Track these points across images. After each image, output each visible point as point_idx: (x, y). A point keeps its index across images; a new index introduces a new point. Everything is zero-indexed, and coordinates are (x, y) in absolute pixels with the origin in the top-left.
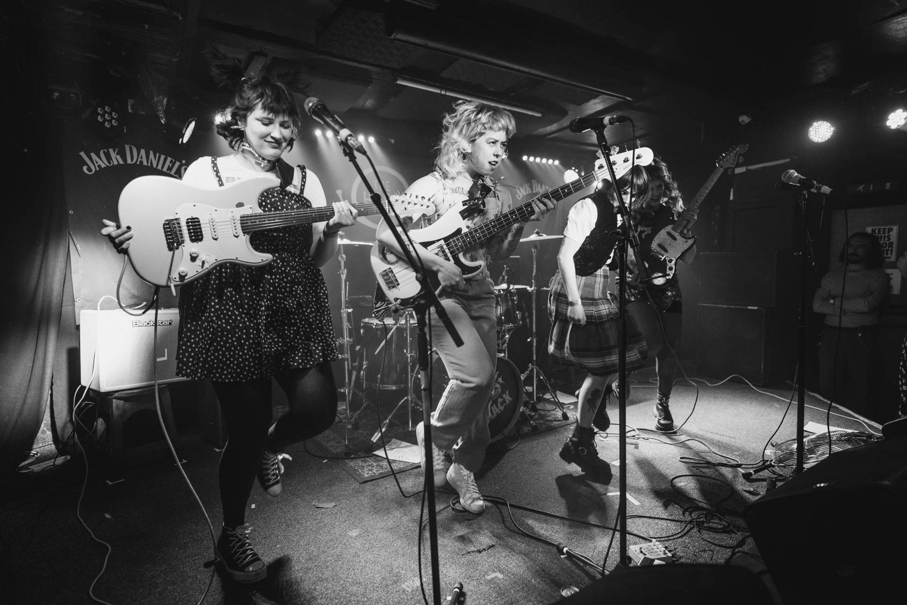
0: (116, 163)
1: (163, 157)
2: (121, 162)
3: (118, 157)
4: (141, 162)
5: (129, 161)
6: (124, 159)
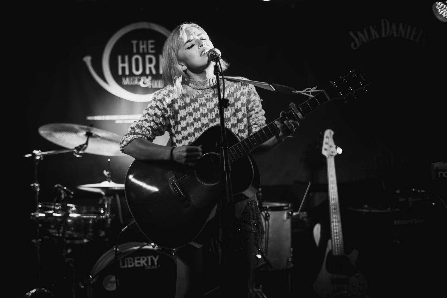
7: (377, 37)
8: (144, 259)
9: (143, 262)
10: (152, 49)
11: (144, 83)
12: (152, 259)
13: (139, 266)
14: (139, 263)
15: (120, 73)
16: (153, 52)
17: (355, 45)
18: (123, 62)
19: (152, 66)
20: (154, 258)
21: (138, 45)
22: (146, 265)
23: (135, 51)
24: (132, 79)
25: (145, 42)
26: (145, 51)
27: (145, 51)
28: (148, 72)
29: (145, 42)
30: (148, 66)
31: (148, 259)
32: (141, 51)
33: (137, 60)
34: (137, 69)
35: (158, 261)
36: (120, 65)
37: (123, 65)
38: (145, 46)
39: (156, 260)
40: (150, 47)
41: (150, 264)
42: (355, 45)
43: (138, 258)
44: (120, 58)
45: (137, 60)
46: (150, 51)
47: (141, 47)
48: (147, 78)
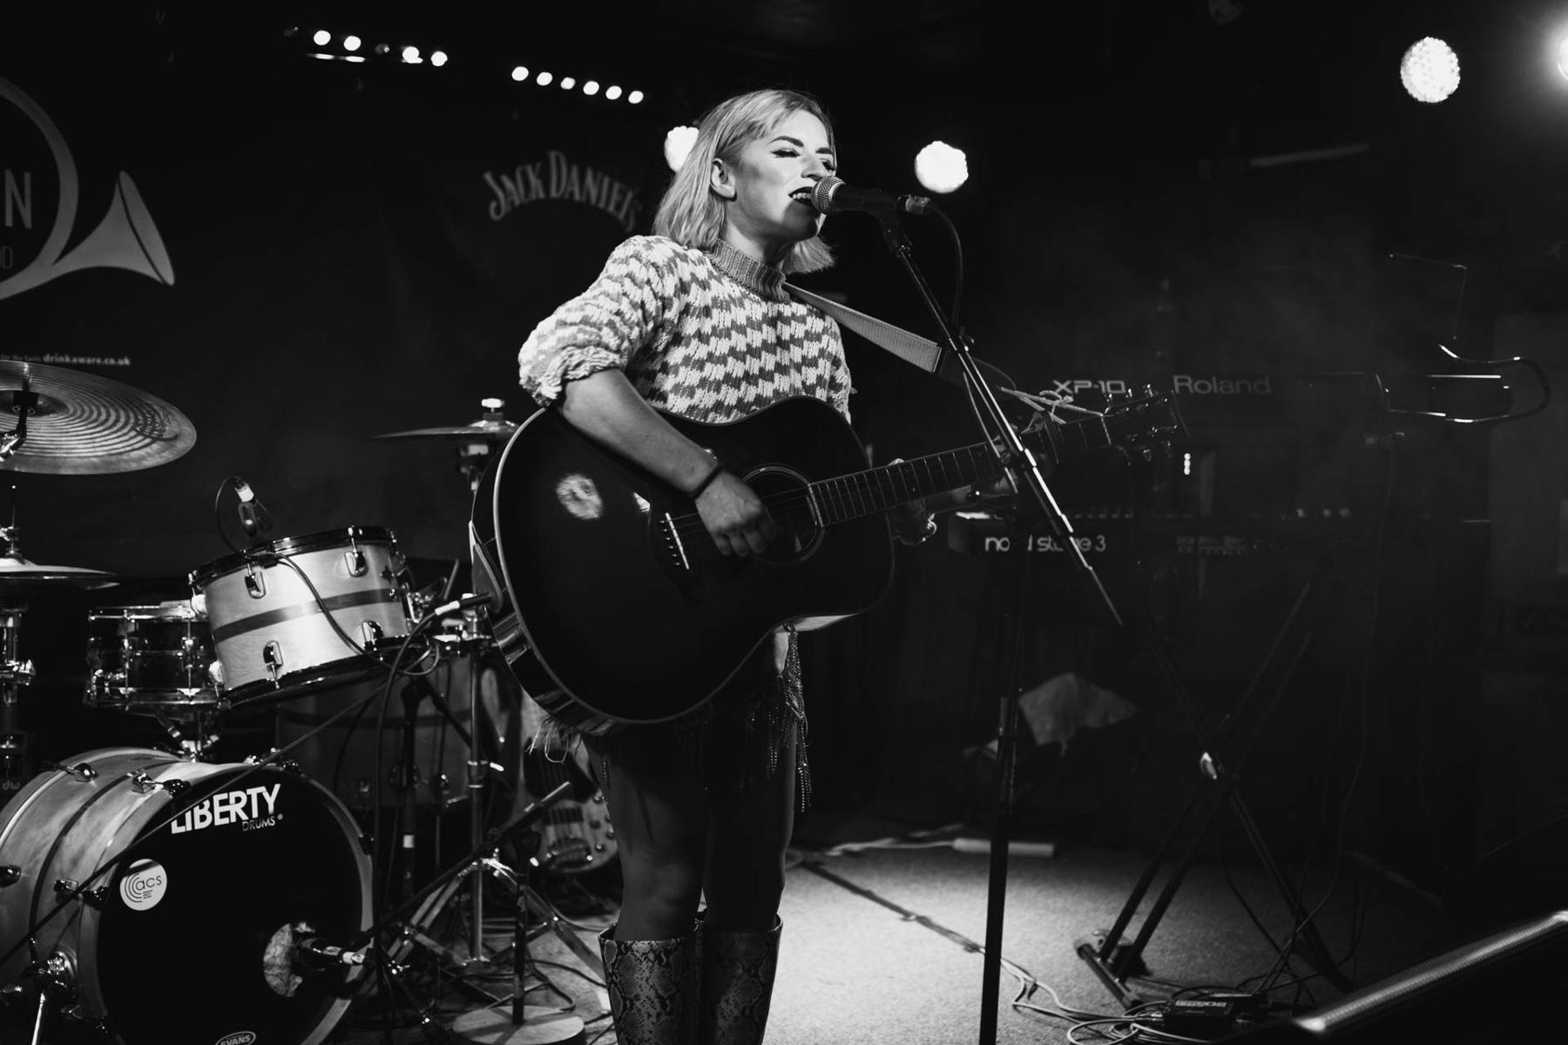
7: (542, 195)
8: (238, 800)
9: (236, 809)
12: (260, 796)
13: (225, 821)
14: (225, 815)
17: (498, 210)
20: (266, 795)
22: (244, 817)
31: (249, 797)
35: (276, 804)
39: (271, 800)
41: (255, 814)
42: (498, 210)
43: (224, 796)
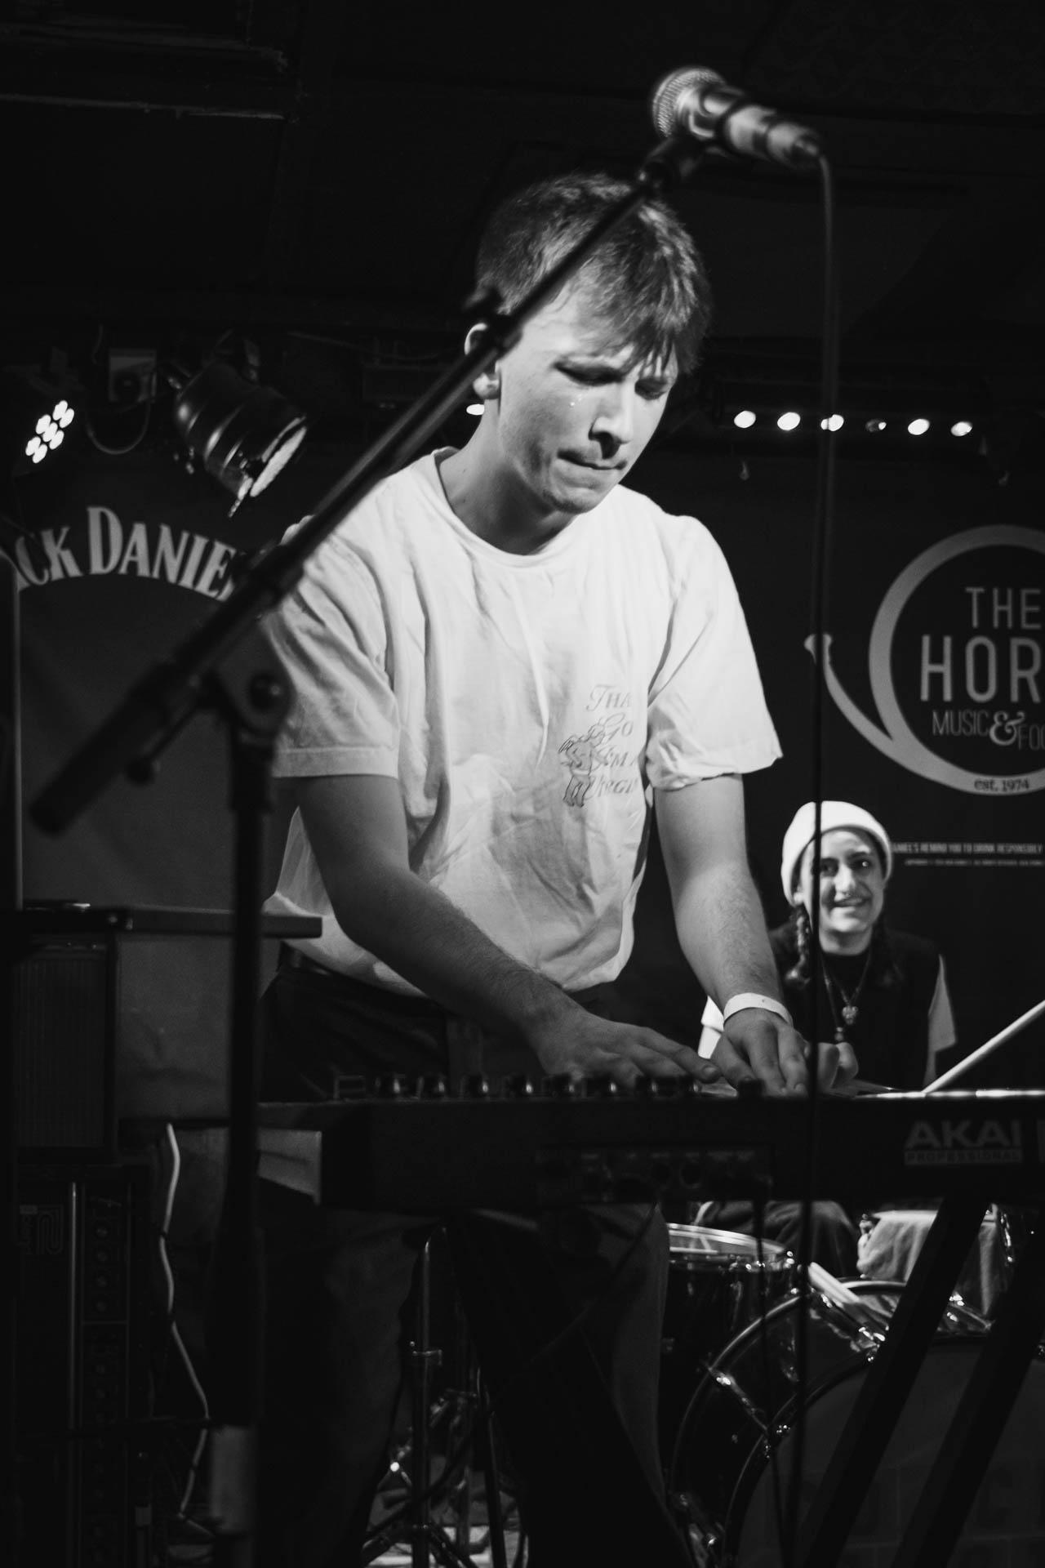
0: (56, 573)
1: (200, 543)
2: (74, 571)
3: (67, 557)
4: (133, 566)
5: (97, 567)
6: (83, 560)
10: (1031, 618)
11: (1000, 733)
15: (925, 696)
16: (1037, 626)
18: (937, 658)
19: (1030, 675)
21: (985, 603)
23: (975, 624)
24: (962, 716)
25: (1010, 592)
26: (1010, 624)
27: (1010, 624)
28: (1015, 697)
29: (1010, 592)
30: (1016, 674)
32: (996, 624)
33: (981, 651)
34: (982, 687)
36: (927, 668)
37: (936, 668)
38: (1009, 608)
40: (1025, 609)
44: (926, 641)
45: (981, 651)
46: (1025, 625)
47: (997, 608)
48: (1013, 717)
